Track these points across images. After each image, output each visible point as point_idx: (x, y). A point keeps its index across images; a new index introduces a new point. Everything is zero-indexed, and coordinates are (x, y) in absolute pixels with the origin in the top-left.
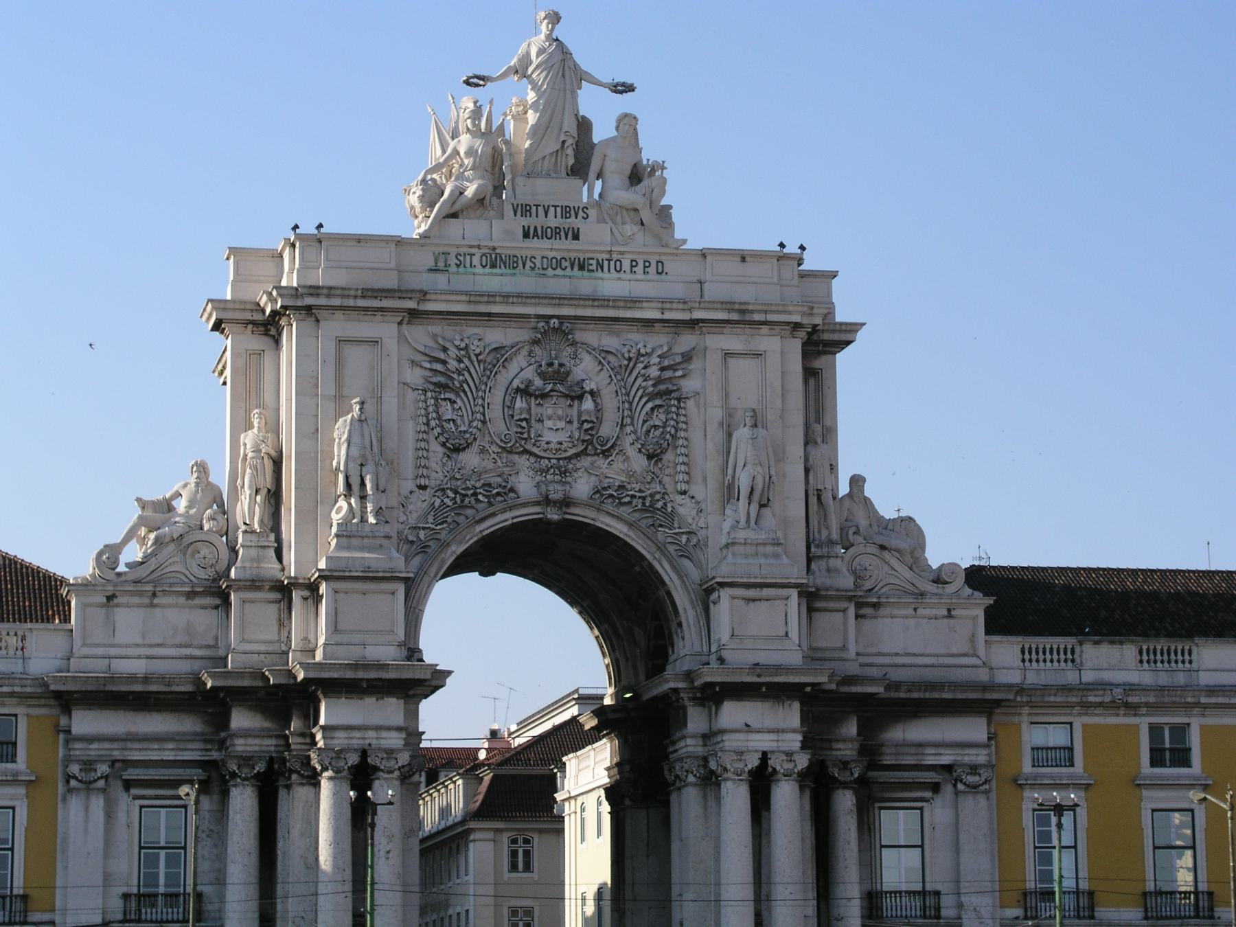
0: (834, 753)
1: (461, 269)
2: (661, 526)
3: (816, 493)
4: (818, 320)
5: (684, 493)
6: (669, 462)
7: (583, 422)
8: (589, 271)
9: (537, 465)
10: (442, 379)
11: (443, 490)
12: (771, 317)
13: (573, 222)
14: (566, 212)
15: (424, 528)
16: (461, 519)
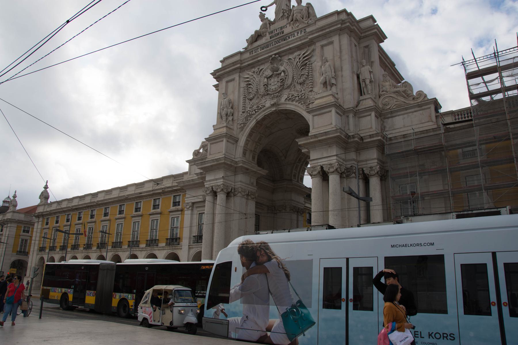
0: (368, 165)
1: (255, 54)
2: (304, 103)
3: (363, 81)
4: (348, 24)
5: (311, 91)
6: (308, 83)
7: (281, 79)
8: (286, 40)
9: (271, 97)
10: (248, 83)
11: (247, 111)
12: (331, 29)
13: (282, 30)
14: (281, 28)
15: (243, 123)
16: (251, 119)
